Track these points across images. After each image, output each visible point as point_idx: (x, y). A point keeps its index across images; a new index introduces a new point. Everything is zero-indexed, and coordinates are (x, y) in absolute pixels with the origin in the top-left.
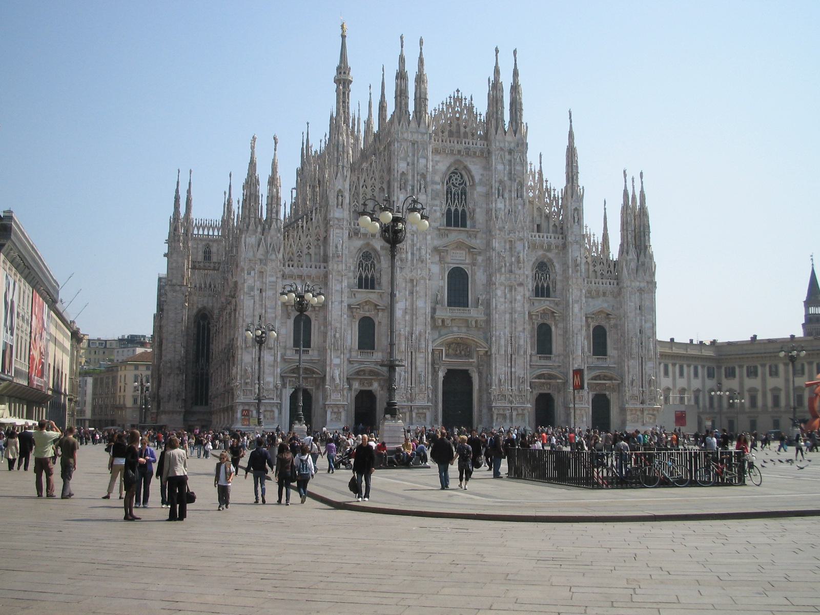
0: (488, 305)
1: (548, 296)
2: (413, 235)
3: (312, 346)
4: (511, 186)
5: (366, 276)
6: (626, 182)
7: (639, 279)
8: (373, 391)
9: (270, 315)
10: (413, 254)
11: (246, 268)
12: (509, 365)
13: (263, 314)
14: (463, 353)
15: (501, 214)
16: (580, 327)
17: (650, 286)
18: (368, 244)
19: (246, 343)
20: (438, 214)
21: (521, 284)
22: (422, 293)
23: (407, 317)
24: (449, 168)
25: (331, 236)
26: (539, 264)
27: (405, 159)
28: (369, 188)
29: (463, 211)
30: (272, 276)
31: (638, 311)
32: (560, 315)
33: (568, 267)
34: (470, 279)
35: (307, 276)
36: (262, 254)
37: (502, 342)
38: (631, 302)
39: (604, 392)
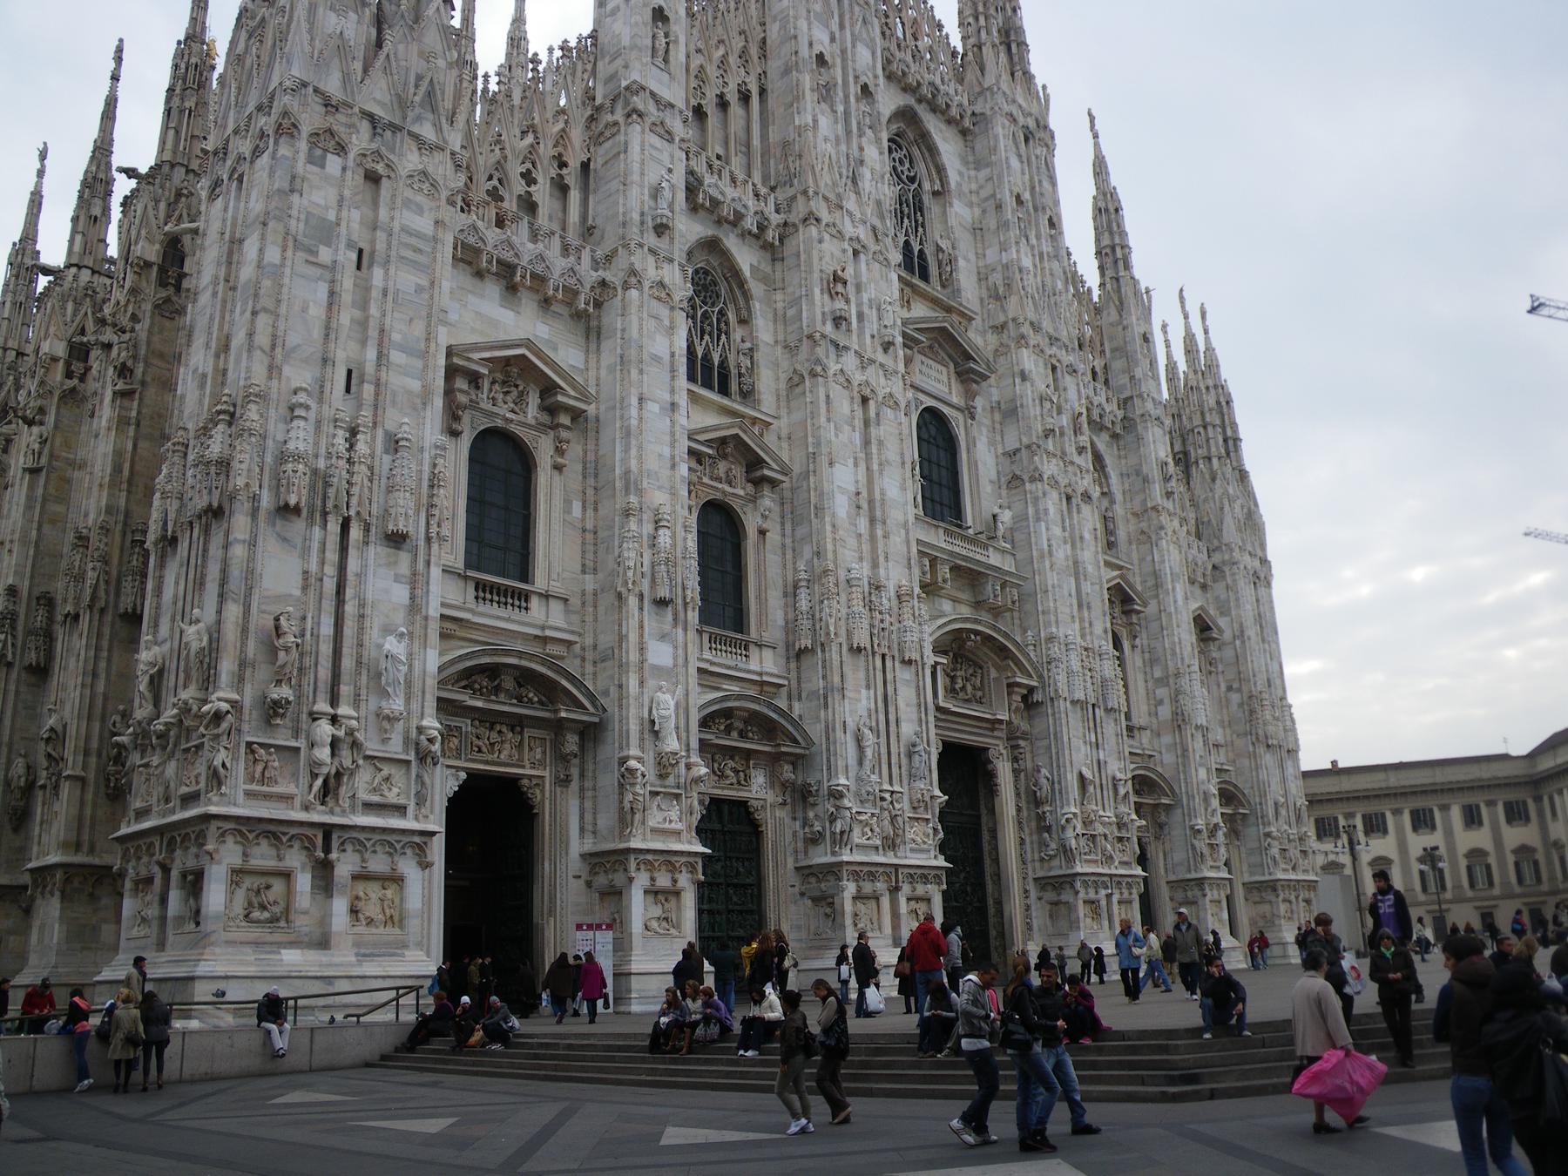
0: (1018, 539)
2: (856, 253)
3: (540, 582)
4: (1037, 225)
5: (707, 357)
6: (1186, 317)
8: (753, 803)
10: (861, 316)
11: (305, 130)
13: (370, 368)
14: (969, 688)
19: (279, 483)
22: (892, 453)
23: (863, 524)
25: (635, 148)
28: (712, 71)
30: (420, 211)
33: (1146, 480)
34: (964, 455)
35: (534, 276)
36: (379, 103)
37: (1076, 664)
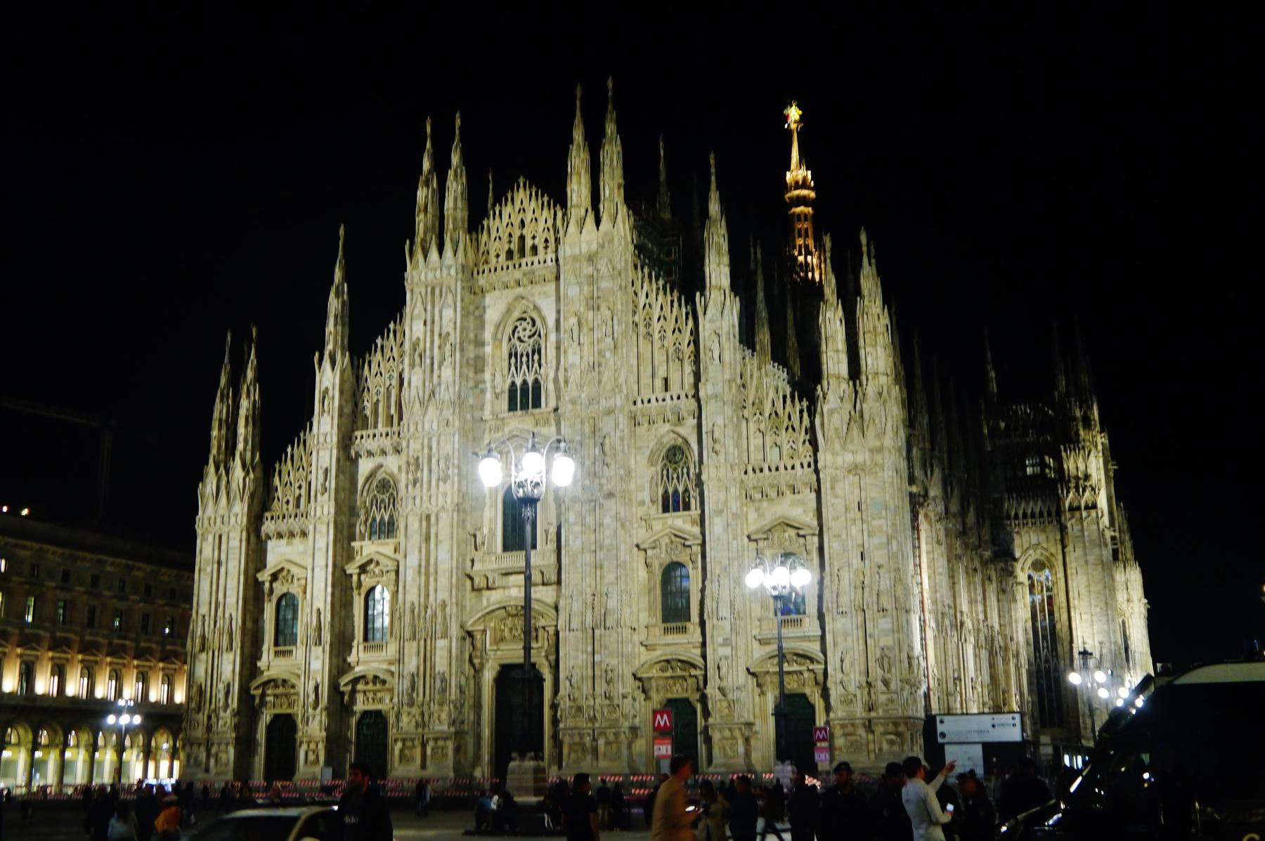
1: (687, 507)
5: (382, 518)
7: (851, 447)
9: (231, 600)
12: (590, 649)
15: (574, 376)
16: (725, 562)
17: (878, 458)
18: (381, 466)
20: (489, 395)
21: (610, 495)
24: (509, 311)
26: (669, 450)
27: (419, 316)
29: (536, 381)
31: (854, 513)
32: (700, 542)
37: (577, 606)
38: (836, 497)
39: (799, 691)
